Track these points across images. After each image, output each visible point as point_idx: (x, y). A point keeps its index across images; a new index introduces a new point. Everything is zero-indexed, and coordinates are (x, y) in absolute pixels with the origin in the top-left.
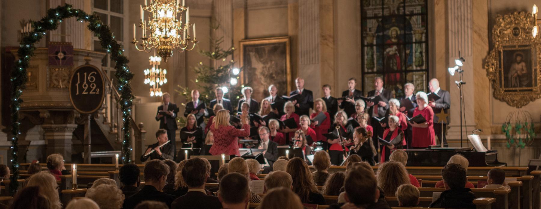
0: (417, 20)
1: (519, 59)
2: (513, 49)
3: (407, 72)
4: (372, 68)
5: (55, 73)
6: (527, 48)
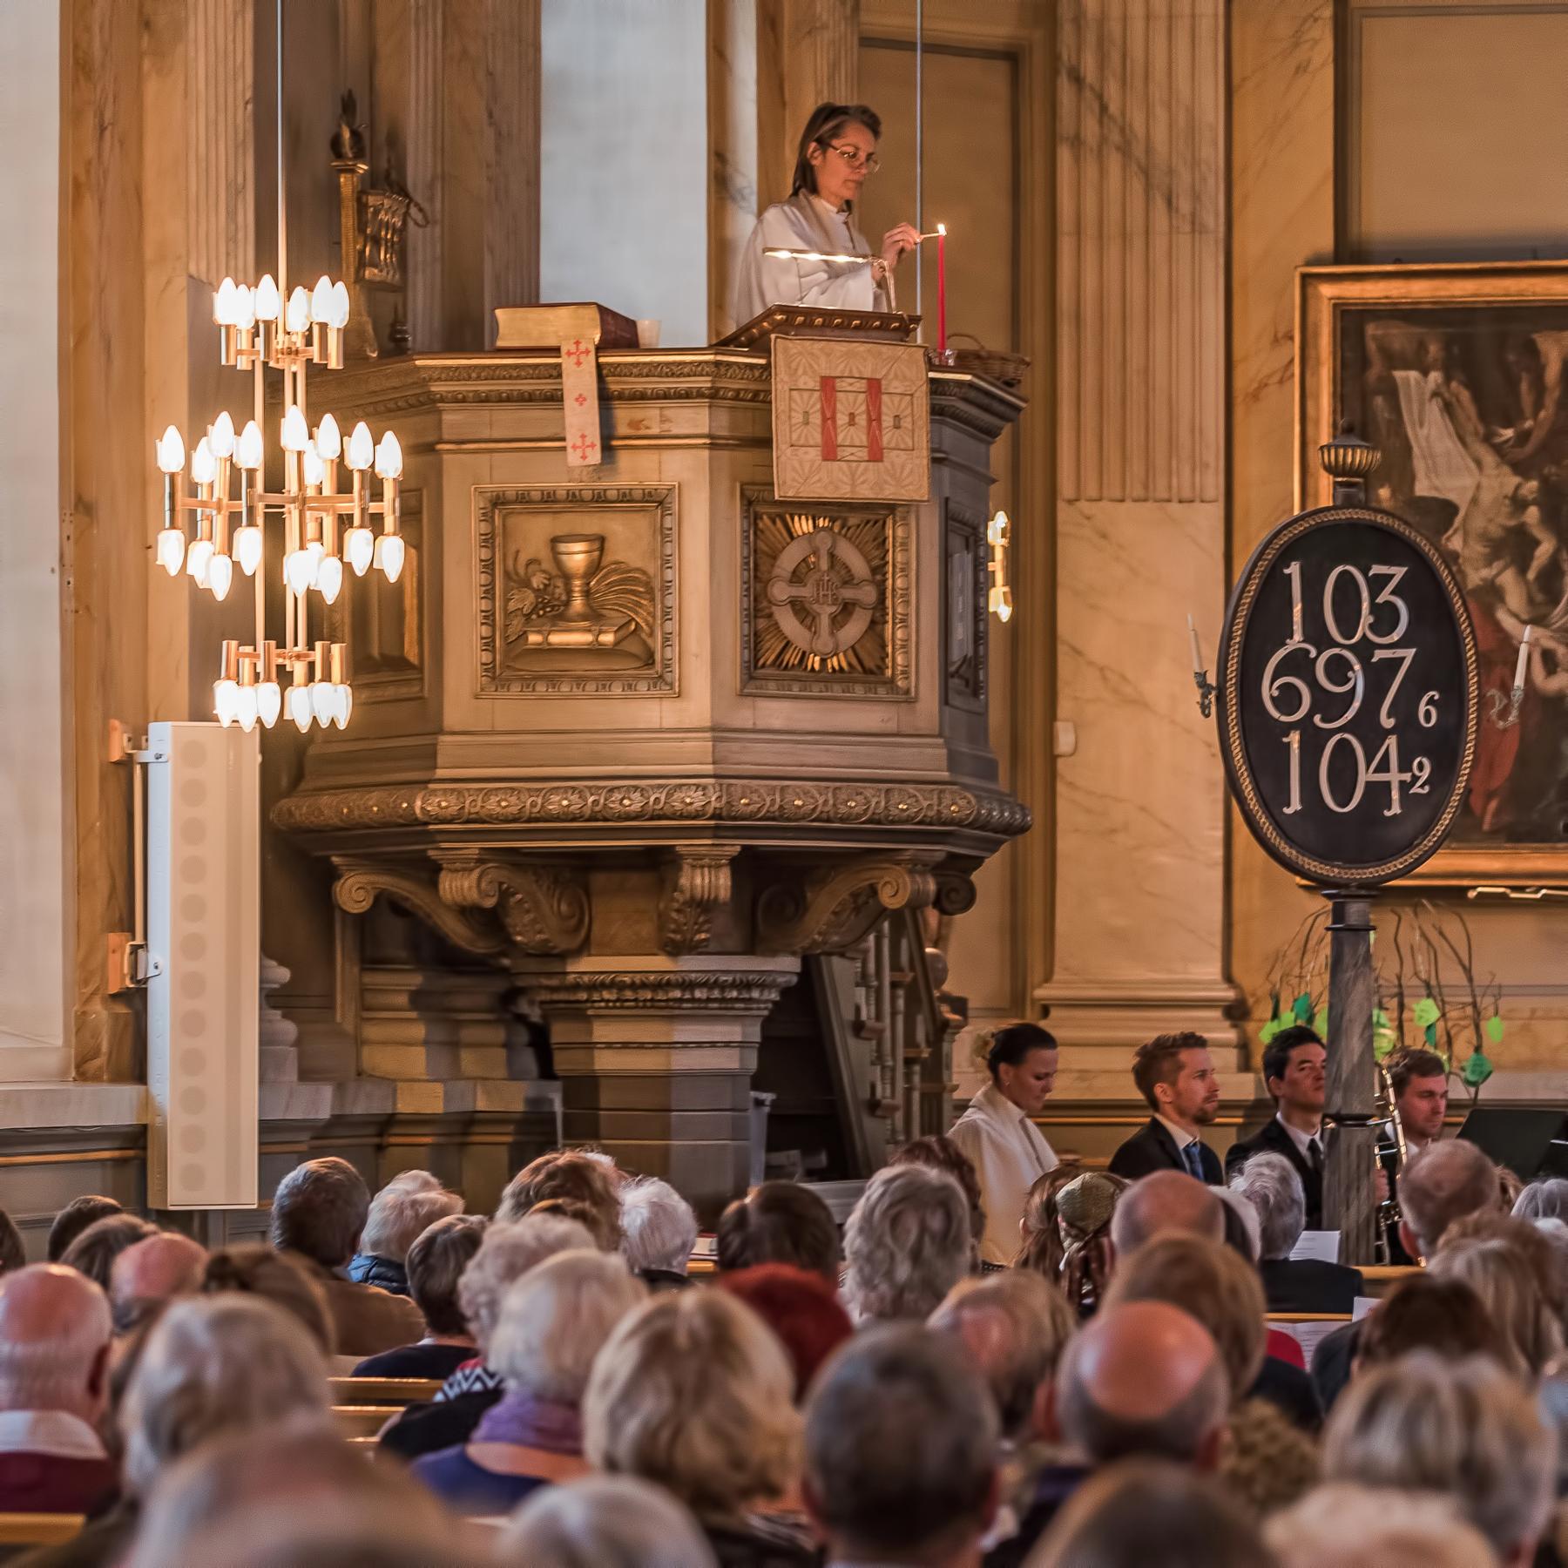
5: (789, 559)
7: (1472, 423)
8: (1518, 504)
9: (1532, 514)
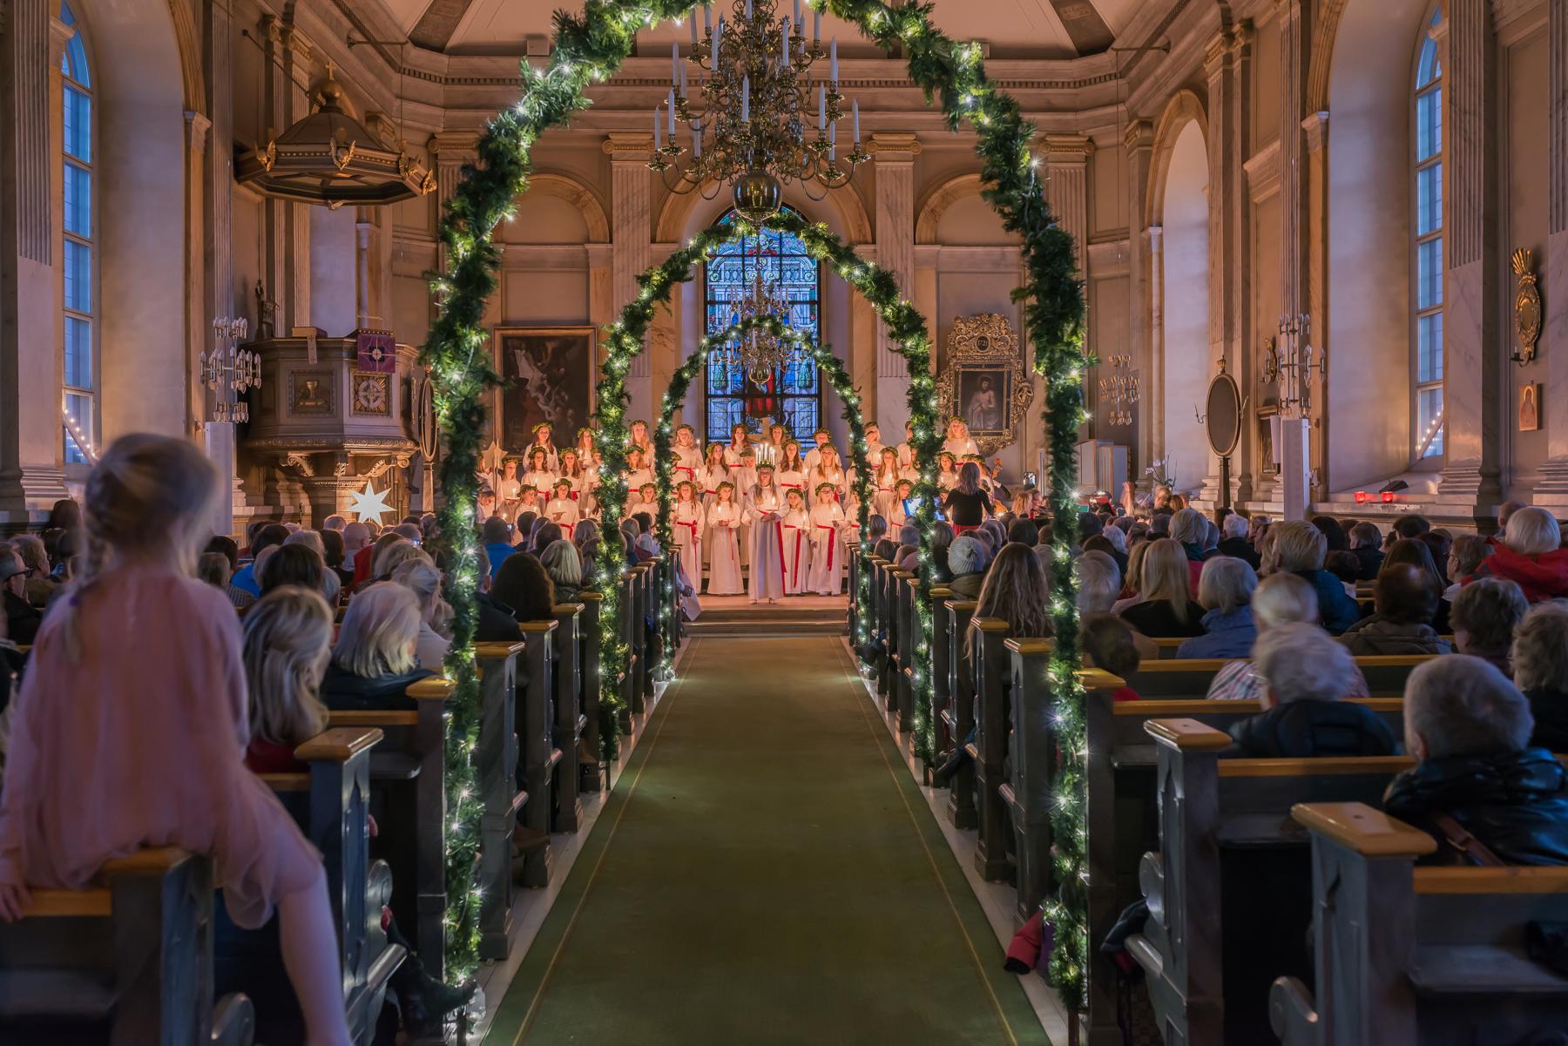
0: (802, 312)
1: (985, 385)
2: (978, 370)
3: (784, 396)
4: (724, 388)
6: (1000, 370)
7: (532, 362)
8: (542, 379)
9: (545, 382)
